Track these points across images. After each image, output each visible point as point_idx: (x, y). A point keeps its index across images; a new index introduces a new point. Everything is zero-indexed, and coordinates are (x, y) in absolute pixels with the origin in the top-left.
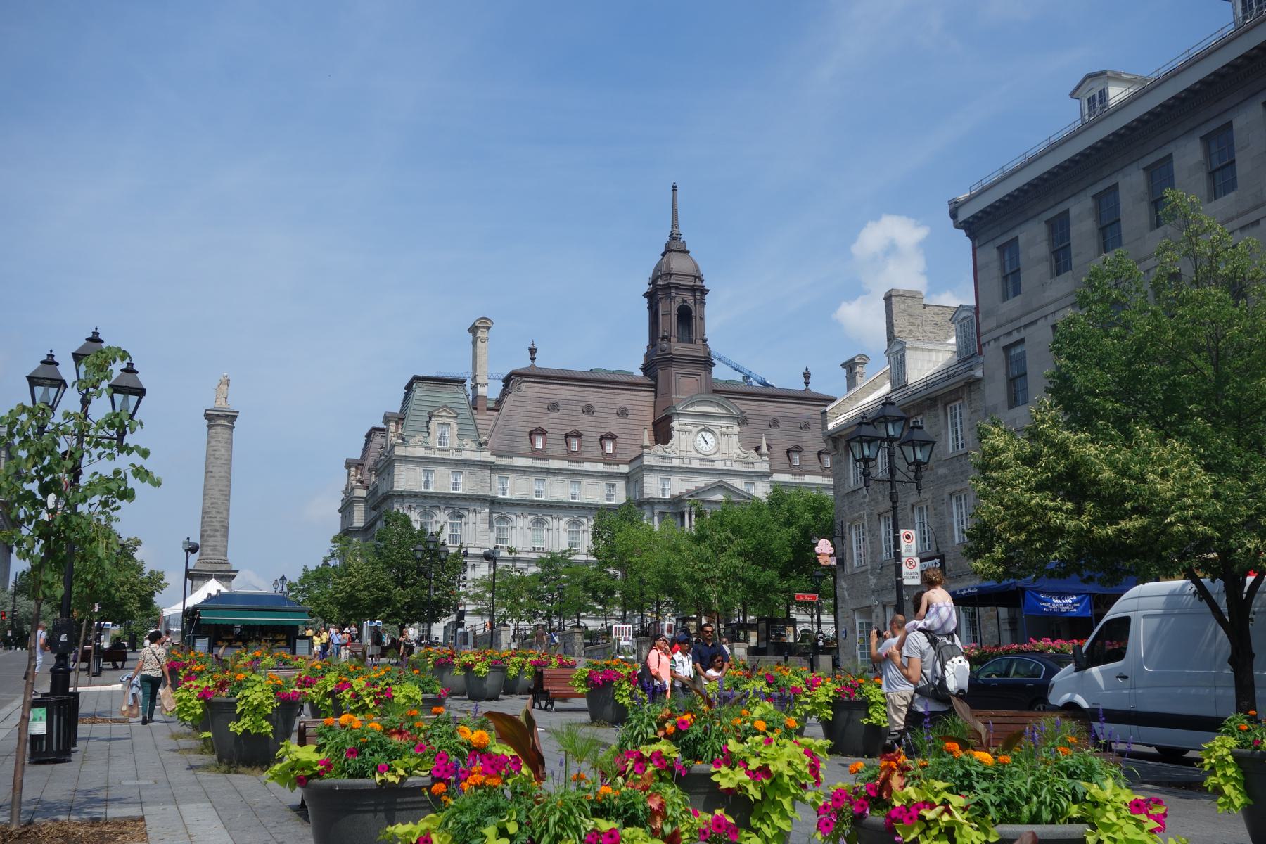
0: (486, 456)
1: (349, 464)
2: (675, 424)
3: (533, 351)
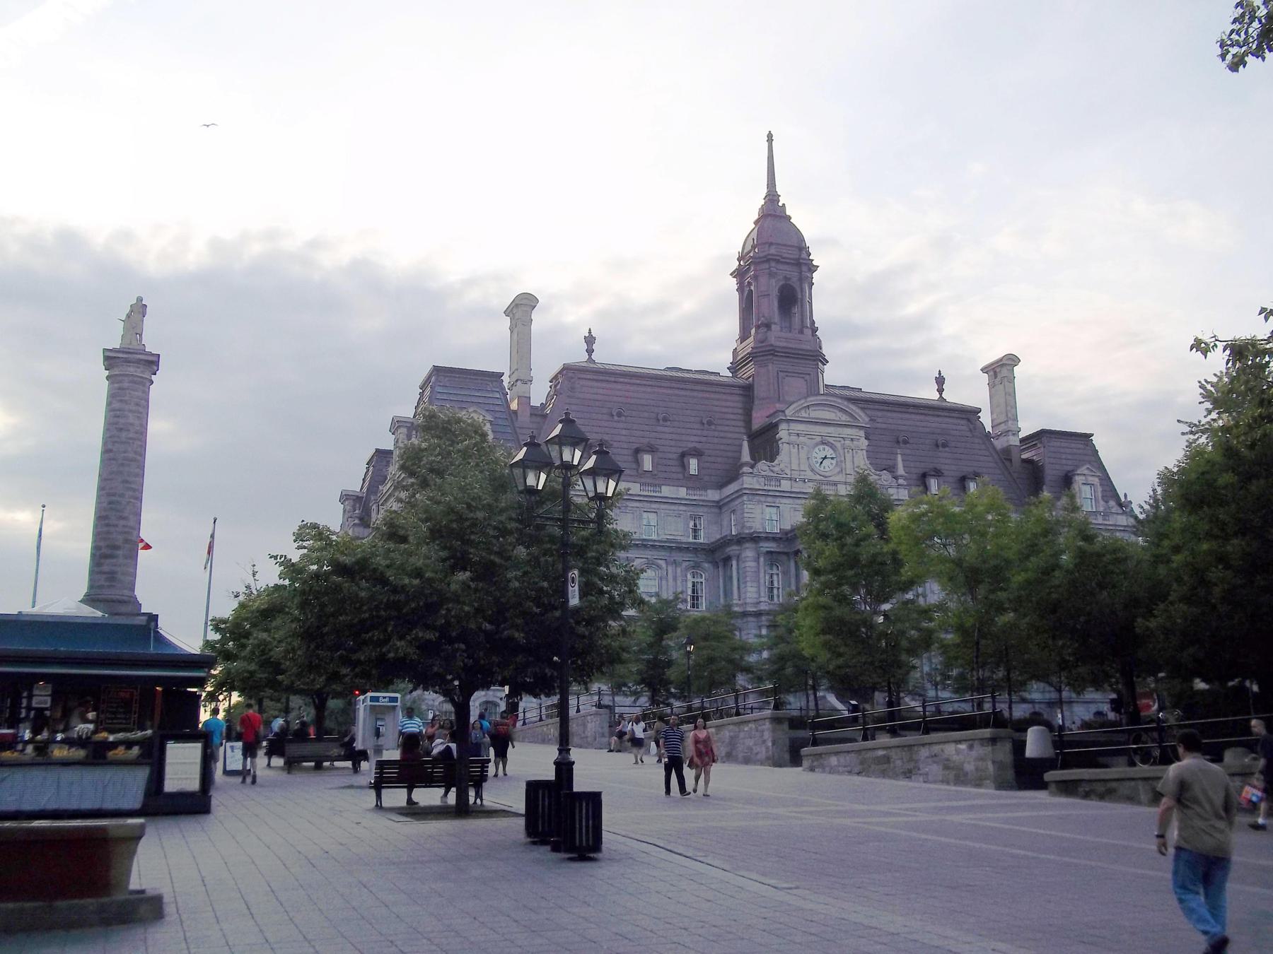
1: (345, 497)
2: (783, 433)
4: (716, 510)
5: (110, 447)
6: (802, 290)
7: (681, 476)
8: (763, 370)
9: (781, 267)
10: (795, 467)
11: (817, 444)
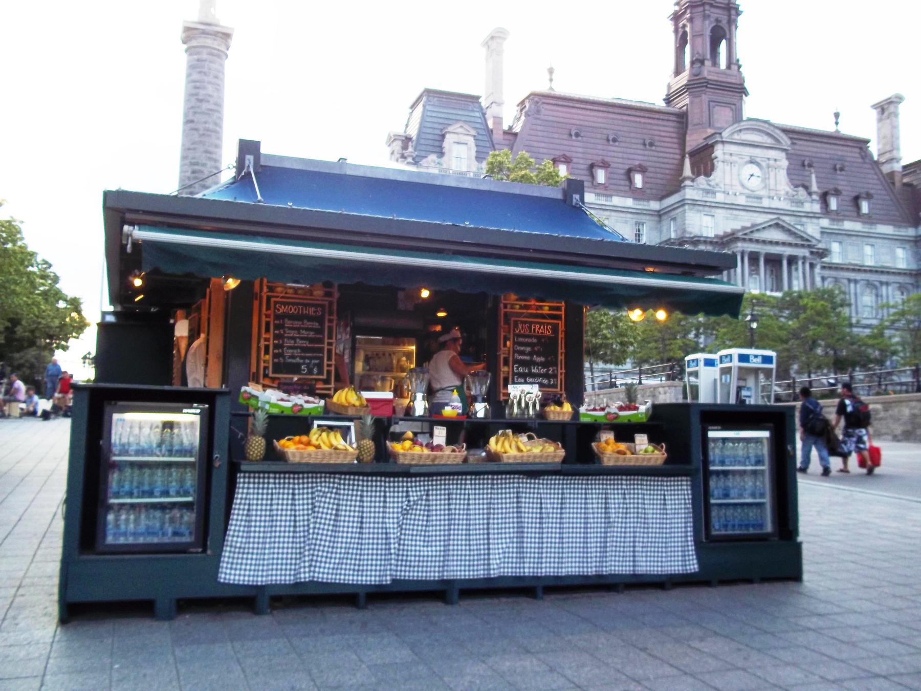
2: (719, 151)
4: (656, 218)
5: (191, 117)
6: (730, 30)
7: (627, 188)
8: (697, 100)
9: (713, 10)
10: (727, 181)
11: (747, 163)
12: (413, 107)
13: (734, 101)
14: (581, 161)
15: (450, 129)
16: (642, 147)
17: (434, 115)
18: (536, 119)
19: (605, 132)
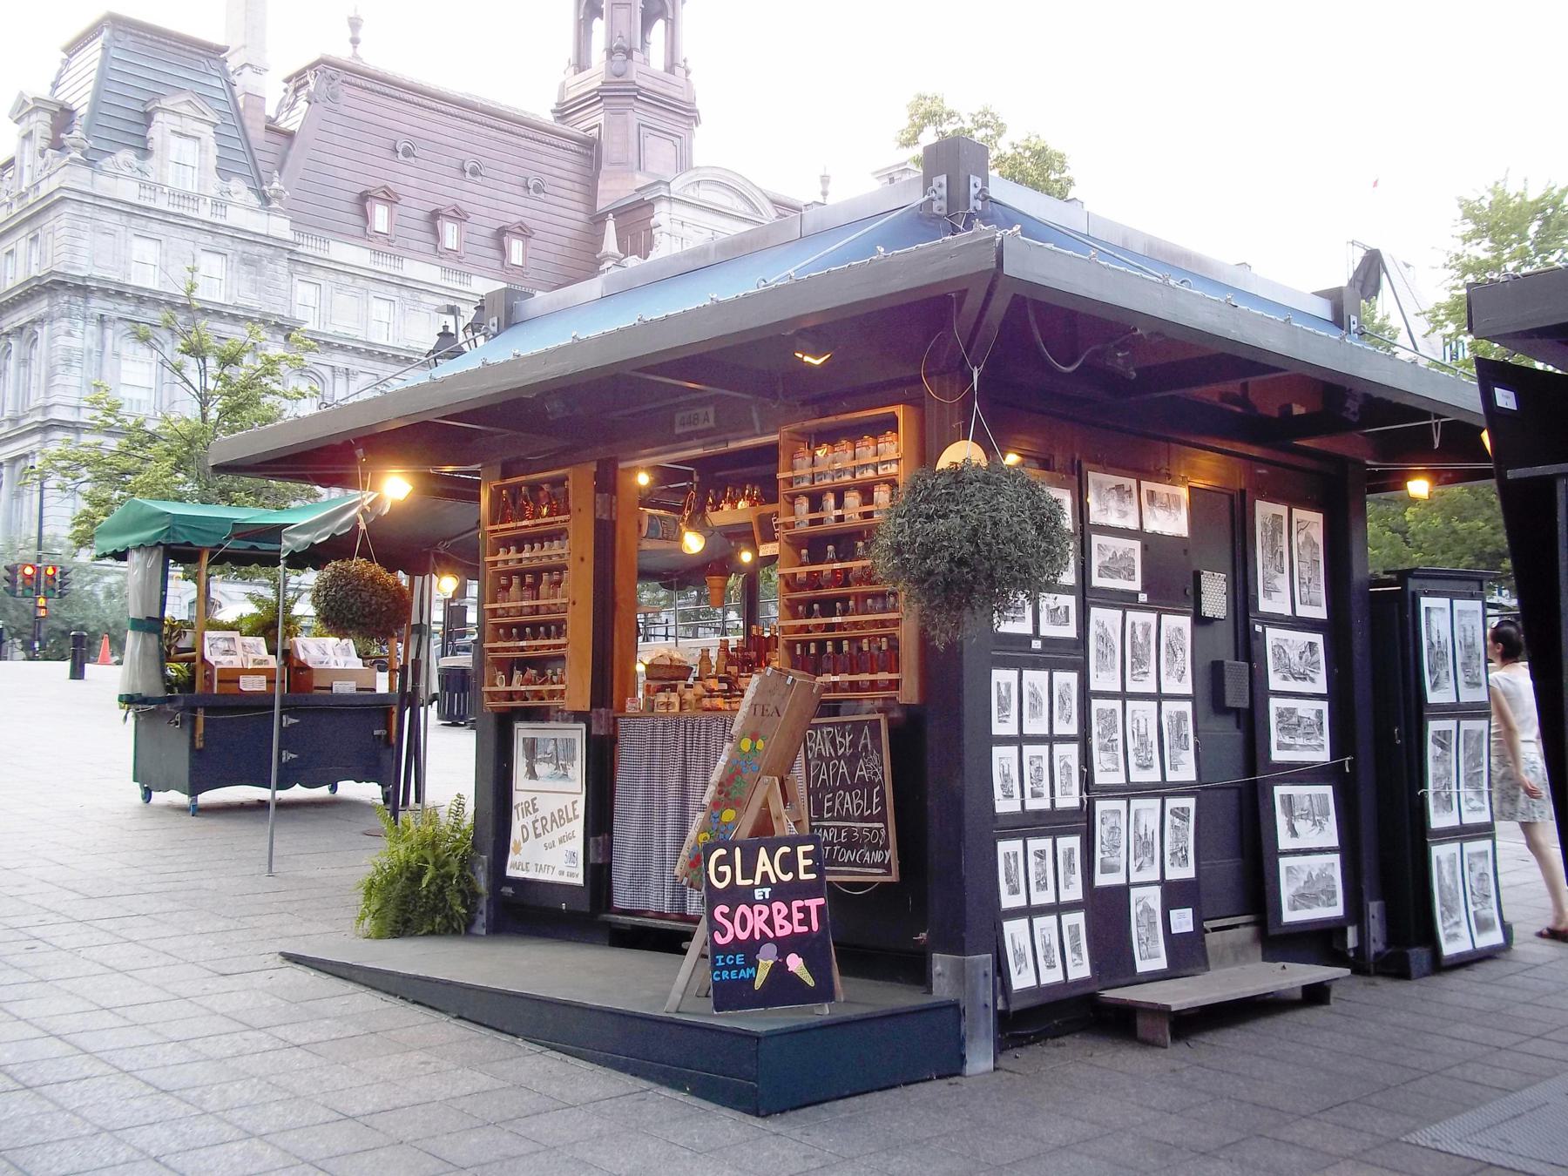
0: (280, 227)
3: (355, 24)
12: (73, 48)
13: (678, 130)
14: (414, 203)
15: (165, 103)
16: (519, 190)
17: (127, 69)
18: (329, 109)
19: (463, 155)
